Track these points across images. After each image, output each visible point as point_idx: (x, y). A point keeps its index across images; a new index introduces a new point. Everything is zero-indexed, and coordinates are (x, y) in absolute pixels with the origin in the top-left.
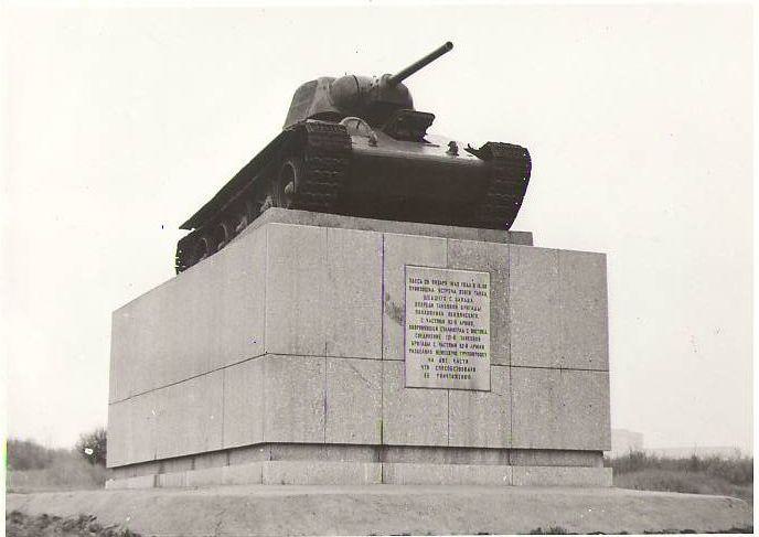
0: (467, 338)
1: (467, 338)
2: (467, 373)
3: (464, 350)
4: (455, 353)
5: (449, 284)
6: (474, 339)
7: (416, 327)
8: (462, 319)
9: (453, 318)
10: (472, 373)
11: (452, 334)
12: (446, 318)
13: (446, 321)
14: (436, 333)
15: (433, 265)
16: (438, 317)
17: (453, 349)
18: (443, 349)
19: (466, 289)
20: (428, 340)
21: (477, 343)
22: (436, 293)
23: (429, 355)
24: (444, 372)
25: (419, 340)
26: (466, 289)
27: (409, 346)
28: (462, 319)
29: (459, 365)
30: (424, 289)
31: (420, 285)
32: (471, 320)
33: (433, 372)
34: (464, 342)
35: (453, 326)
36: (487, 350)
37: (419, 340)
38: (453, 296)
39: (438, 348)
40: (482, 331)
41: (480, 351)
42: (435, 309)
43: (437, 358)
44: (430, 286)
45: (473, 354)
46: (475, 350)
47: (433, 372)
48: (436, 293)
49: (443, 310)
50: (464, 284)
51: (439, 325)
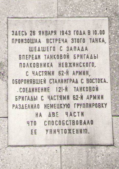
0: (82, 89)
1: (82, 89)
2: (84, 127)
3: (79, 101)
4: (68, 106)
5: (58, 33)
6: (90, 89)
7: (20, 81)
8: (76, 69)
9: (64, 69)
10: (88, 126)
11: (64, 85)
12: (55, 68)
13: (56, 73)
14: (44, 86)
15: (42, 15)
16: (47, 69)
17: (65, 102)
18: (53, 102)
19: (79, 37)
20: (35, 94)
21: (95, 93)
22: (44, 44)
23: (36, 110)
24: (54, 127)
25: (24, 94)
26: (79, 37)
27: (12, 101)
28: (76, 69)
29: (72, 118)
30: (28, 41)
31: (24, 37)
32: (86, 69)
33: (40, 127)
34: (79, 93)
35: (65, 77)
36: (107, 99)
37: (24, 94)
38: (64, 46)
39: (46, 101)
40: (100, 81)
41: (101, 101)
42: (42, 60)
43: (45, 113)
44: (37, 36)
45: (90, 105)
46: (92, 101)
47: (40, 127)
48: (44, 44)
49: (53, 61)
50: (77, 32)
51: (47, 78)
